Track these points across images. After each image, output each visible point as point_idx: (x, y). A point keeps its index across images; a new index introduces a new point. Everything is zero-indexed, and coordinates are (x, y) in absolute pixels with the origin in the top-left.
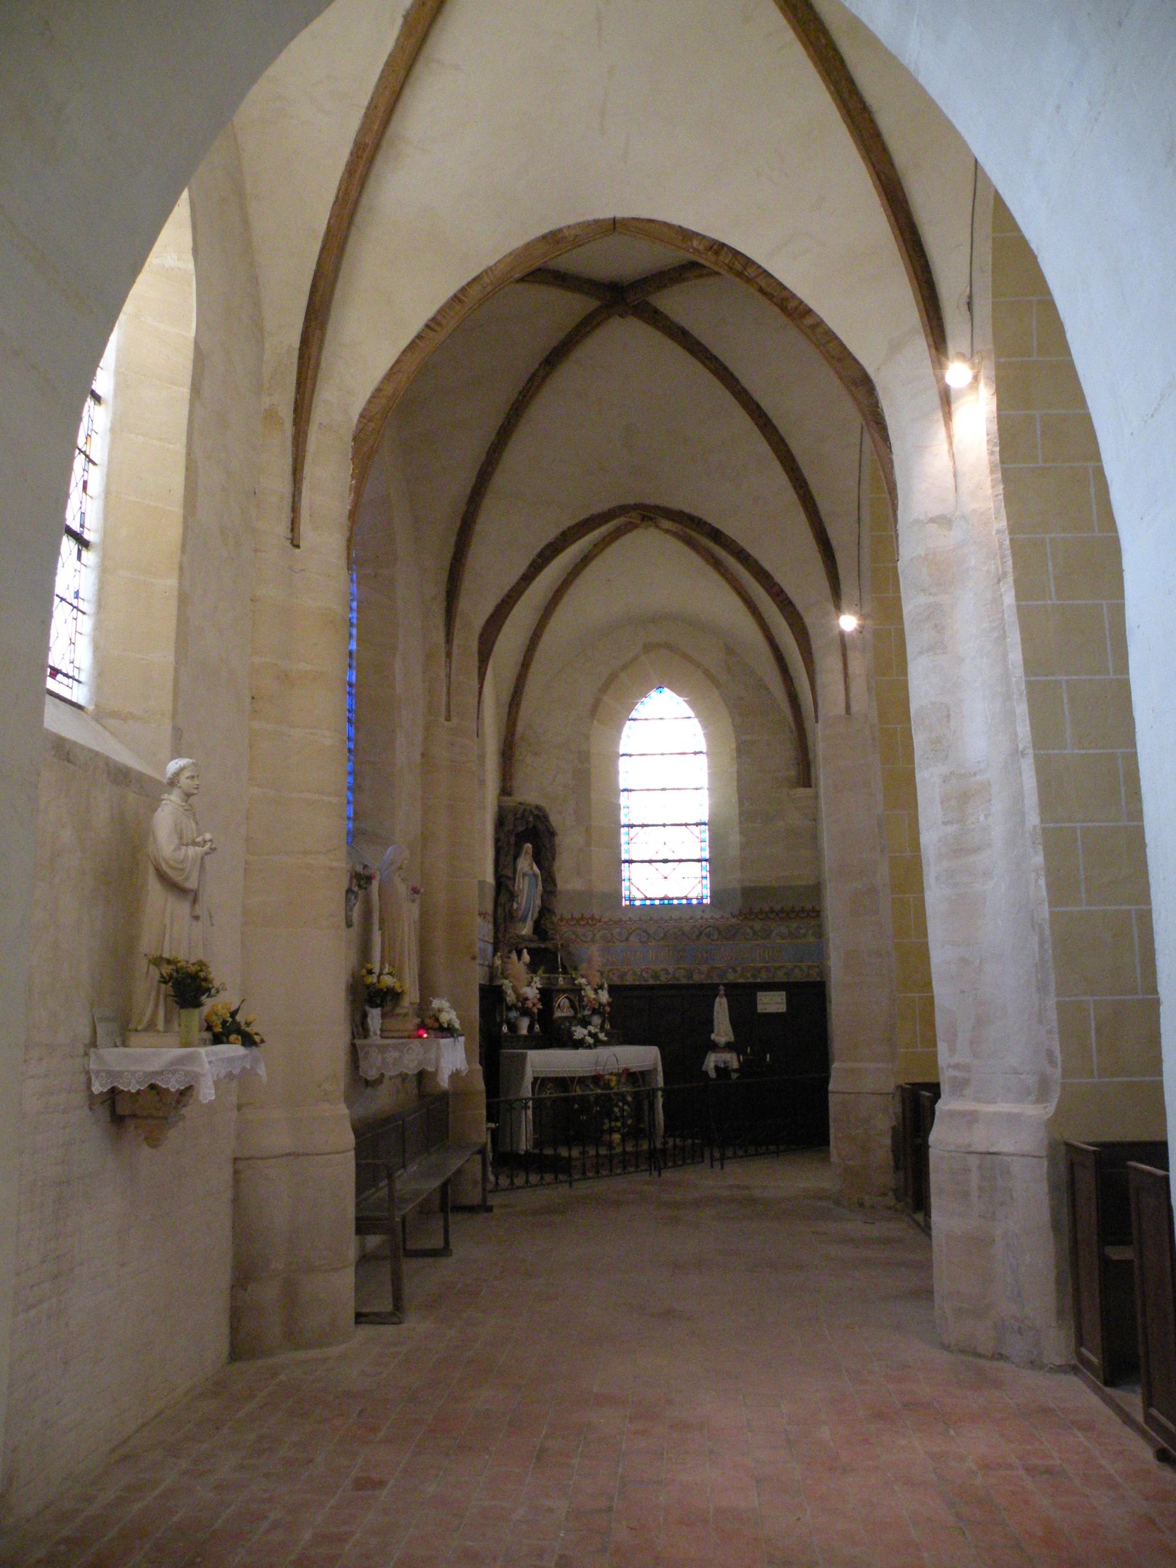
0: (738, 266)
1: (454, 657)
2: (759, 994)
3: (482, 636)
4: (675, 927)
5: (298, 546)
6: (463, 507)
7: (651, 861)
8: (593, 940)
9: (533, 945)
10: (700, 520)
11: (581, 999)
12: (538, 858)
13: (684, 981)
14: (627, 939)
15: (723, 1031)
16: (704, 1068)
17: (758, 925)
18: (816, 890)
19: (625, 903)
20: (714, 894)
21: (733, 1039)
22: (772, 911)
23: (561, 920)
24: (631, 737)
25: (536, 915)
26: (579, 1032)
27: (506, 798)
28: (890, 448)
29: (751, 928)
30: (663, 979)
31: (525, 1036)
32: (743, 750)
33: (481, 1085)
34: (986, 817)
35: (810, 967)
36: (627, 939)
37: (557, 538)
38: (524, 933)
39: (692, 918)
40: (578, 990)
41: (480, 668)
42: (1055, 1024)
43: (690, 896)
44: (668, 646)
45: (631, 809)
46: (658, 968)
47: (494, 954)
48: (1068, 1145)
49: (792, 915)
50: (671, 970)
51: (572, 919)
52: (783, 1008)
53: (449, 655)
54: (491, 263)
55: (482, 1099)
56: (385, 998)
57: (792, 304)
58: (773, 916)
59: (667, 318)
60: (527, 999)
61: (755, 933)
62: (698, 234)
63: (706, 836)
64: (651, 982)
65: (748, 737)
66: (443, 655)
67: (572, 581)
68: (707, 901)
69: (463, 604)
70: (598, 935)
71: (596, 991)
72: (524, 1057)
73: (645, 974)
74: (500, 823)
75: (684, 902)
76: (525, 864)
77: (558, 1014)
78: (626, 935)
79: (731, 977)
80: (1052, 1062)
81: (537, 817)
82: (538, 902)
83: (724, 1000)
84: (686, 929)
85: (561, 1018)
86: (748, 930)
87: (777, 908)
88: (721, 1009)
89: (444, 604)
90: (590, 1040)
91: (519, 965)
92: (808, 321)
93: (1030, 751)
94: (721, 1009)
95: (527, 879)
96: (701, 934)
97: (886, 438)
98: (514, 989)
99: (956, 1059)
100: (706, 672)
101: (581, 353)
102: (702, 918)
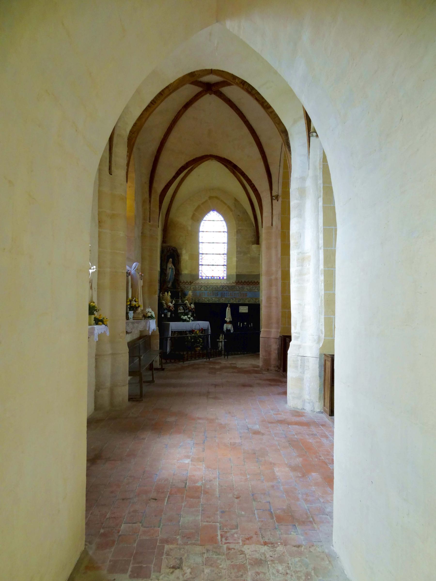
0: (250, 90)
5: (111, 175)
7: (208, 265)
8: (190, 289)
11: (186, 307)
12: (174, 263)
13: (218, 302)
15: (228, 317)
17: (240, 286)
18: (258, 276)
19: (200, 278)
20: (227, 276)
21: (231, 320)
22: (245, 282)
26: (185, 317)
27: (164, 244)
28: (291, 154)
29: (239, 287)
32: (238, 232)
34: (309, 265)
37: (185, 165)
38: (169, 286)
40: (186, 304)
41: (159, 206)
42: (323, 323)
44: (216, 198)
45: (203, 248)
47: (160, 293)
48: (325, 355)
50: (213, 299)
54: (172, 82)
55: (158, 338)
57: (265, 104)
59: (224, 95)
60: (170, 307)
62: (238, 78)
63: (226, 258)
65: (240, 228)
66: (148, 201)
69: (155, 185)
70: (192, 287)
71: (190, 305)
72: (169, 324)
74: (162, 252)
75: (218, 278)
76: (170, 265)
77: (179, 311)
79: (232, 301)
80: (322, 333)
81: (173, 250)
82: (174, 277)
84: (218, 287)
87: (247, 281)
90: (188, 319)
91: (168, 295)
92: (270, 110)
93: (323, 248)
95: (170, 270)
97: (290, 150)
99: (296, 331)
100: (229, 207)
101: (196, 104)
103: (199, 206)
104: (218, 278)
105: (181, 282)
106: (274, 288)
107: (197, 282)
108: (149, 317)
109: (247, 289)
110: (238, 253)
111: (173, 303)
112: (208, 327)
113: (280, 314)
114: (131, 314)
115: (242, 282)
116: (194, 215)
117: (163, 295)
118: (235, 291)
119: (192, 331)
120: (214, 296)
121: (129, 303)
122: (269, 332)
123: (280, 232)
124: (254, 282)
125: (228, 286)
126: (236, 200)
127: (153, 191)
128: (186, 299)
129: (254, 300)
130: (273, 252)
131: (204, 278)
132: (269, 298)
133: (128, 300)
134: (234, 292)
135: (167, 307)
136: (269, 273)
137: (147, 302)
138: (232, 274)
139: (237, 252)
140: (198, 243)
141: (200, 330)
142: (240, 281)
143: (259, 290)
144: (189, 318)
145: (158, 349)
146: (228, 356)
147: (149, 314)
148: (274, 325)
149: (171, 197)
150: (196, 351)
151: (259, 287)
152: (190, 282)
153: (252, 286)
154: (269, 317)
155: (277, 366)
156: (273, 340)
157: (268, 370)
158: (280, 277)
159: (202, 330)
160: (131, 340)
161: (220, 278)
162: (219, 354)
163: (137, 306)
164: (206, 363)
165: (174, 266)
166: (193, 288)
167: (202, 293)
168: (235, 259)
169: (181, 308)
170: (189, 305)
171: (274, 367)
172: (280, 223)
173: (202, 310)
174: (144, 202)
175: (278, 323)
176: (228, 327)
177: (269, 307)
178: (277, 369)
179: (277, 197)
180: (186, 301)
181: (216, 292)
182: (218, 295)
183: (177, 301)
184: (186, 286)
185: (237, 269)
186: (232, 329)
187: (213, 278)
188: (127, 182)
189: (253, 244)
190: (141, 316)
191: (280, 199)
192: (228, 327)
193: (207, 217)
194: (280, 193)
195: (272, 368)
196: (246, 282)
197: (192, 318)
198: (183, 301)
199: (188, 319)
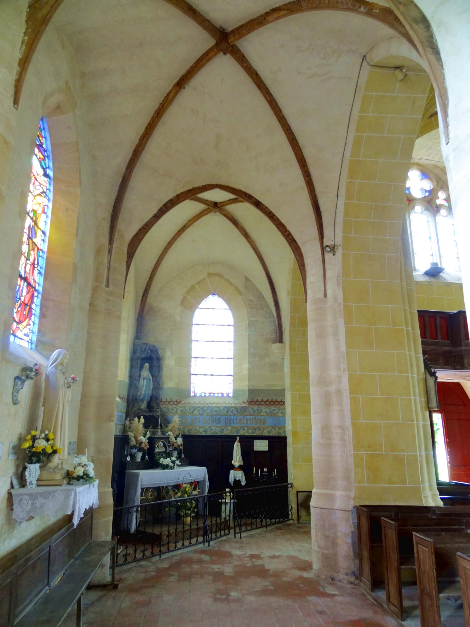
1: (113, 252)
2: (255, 441)
3: (129, 245)
4: (216, 407)
6: (124, 169)
9: (147, 414)
10: (250, 195)
11: (169, 442)
13: (219, 434)
14: (193, 412)
15: (237, 460)
17: (255, 408)
18: (282, 392)
19: (192, 394)
20: (235, 392)
21: (242, 463)
22: (262, 401)
24: (199, 315)
25: (149, 399)
29: (252, 409)
32: (251, 325)
33: (111, 501)
38: (142, 407)
39: (224, 403)
41: (127, 262)
44: (219, 275)
45: (196, 349)
47: (126, 419)
50: (213, 428)
51: (166, 401)
52: (266, 449)
53: (110, 251)
56: (41, 457)
58: (262, 403)
60: (142, 443)
61: (254, 411)
64: (204, 434)
66: (107, 251)
67: (177, 239)
68: (231, 395)
69: (120, 225)
70: (179, 410)
71: (176, 438)
72: (137, 475)
73: (201, 430)
74: (134, 352)
75: (220, 395)
78: (192, 410)
79: (242, 433)
81: (152, 351)
82: (150, 392)
83: (239, 444)
84: (221, 408)
85: (158, 452)
86: (251, 410)
87: (265, 399)
88: (237, 448)
89: (109, 224)
90: (171, 464)
91: (139, 424)
94: (237, 448)
95: (145, 381)
96: (228, 411)
98: (135, 438)
100: (236, 288)
101: (199, 79)
103: (192, 287)
104: (220, 395)
105: (161, 401)
106: (335, 408)
107: (187, 401)
108: (79, 478)
109: (266, 412)
110: (252, 356)
111: (148, 435)
112: (205, 478)
113: (351, 461)
114: (33, 471)
115: (257, 401)
116: (184, 299)
117: (131, 423)
118: (247, 415)
119: (177, 487)
120: (214, 424)
121: (27, 445)
122: (331, 498)
123: (342, 308)
124: (277, 401)
125: (236, 408)
126: (247, 279)
127: (116, 235)
128: (169, 428)
129: (277, 430)
130: (330, 342)
131: (198, 395)
132: (326, 429)
133: (29, 437)
134: (246, 418)
135: (137, 443)
136: (323, 381)
137: (91, 436)
138: (242, 388)
139: (249, 354)
140: (189, 341)
141: (191, 483)
142: (255, 400)
143: (284, 414)
144: (174, 462)
145: (109, 538)
146: (240, 533)
147: (80, 471)
148: (340, 483)
149: (151, 271)
150: (184, 524)
151: (284, 409)
152: (177, 401)
153: (273, 408)
154: (328, 467)
155: (354, 573)
156: (339, 514)
157: (333, 579)
158: (347, 388)
159: (196, 484)
160: (40, 530)
161: (223, 394)
162: (225, 527)
163: (49, 451)
164: (205, 557)
165: (152, 376)
166: (182, 411)
167: (196, 418)
168: (246, 366)
169: (161, 444)
170: (174, 440)
171: (347, 574)
172: (341, 292)
174: (98, 251)
175: (347, 478)
176: (236, 475)
177: (327, 445)
178: (352, 579)
179: (333, 249)
180: (170, 433)
181: (218, 417)
182: (220, 422)
183: (154, 431)
184: (170, 407)
185: (249, 380)
186: (244, 479)
187: (212, 395)
188: (16, 102)
189: (274, 342)
190: (58, 477)
191: (339, 252)
192: (236, 475)
193: (204, 304)
194: (339, 240)
195: (341, 576)
196: (265, 402)
197: (178, 462)
198: (163, 433)
199: (171, 464)
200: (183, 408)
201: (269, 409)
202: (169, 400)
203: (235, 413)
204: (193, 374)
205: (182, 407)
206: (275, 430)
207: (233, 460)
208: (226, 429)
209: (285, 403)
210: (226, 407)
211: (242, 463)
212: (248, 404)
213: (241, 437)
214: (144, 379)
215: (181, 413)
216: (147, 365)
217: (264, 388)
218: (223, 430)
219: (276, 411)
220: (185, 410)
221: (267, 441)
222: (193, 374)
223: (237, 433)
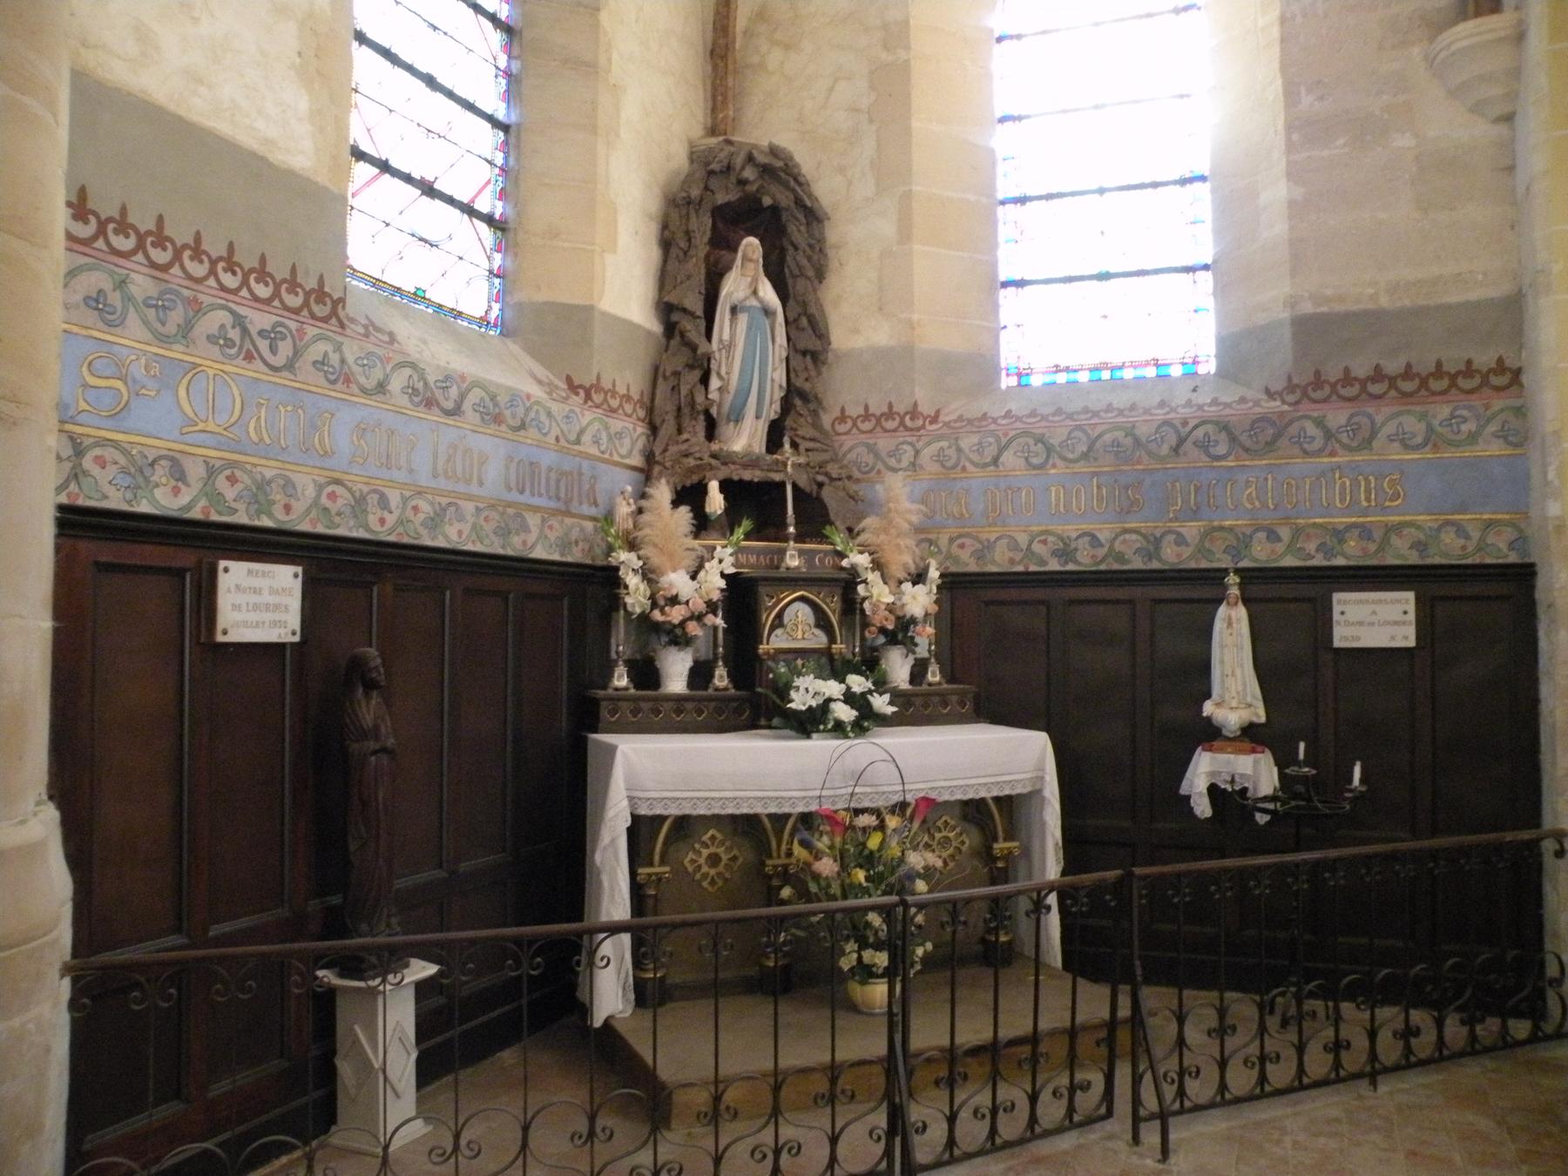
2: (1336, 596)
4: (1116, 427)
13: (1137, 564)
14: (995, 461)
15: (1235, 694)
16: (1184, 790)
17: (1337, 417)
19: (1007, 382)
20: (1228, 347)
21: (1262, 718)
22: (1378, 375)
23: (842, 418)
25: (772, 410)
29: (1319, 423)
30: (1085, 560)
31: (678, 699)
35: (1490, 524)
36: (995, 461)
38: (738, 446)
39: (1162, 404)
43: (1163, 356)
46: (1071, 530)
49: (1436, 385)
51: (867, 416)
52: (1404, 636)
58: (1375, 389)
61: (1329, 435)
64: (1054, 565)
68: (1209, 367)
70: (927, 452)
73: (1037, 547)
75: (1151, 372)
77: (777, 641)
78: (990, 452)
79: (1261, 554)
81: (766, 171)
82: (780, 376)
83: (1241, 613)
84: (1143, 431)
86: (1311, 429)
87: (1393, 366)
88: (1231, 635)
90: (844, 713)
94: (1231, 635)
95: (743, 319)
96: (1181, 441)
98: (649, 574)
102: (1189, 403)
125: (1224, 427)
138: (1261, 319)
142: (1333, 373)
153: (1446, 411)
166: (939, 458)
173: (1008, 638)
184: (884, 443)
196: (1392, 381)
200: (944, 444)
201: (1423, 417)
202: (877, 408)
203: (1221, 449)
204: (1005, 285)
205: (941, 438)
206: (1461, 530)
207: (1208, 696)
208: (1172, 537)
209: (1524, 379)
210: (1166, 423)
211: (1262, 718)
212: (1291, 398)
213: (1249, 577)
214: (734, 310)
215: (936, 468)
216: (751, 245)
217: (1384, 302)
218: (1157, 542)
219: (1470, 426)
220: (959, 450)
221: (1410, 596)
222: (1005, 285)
223: (1237, 556)
